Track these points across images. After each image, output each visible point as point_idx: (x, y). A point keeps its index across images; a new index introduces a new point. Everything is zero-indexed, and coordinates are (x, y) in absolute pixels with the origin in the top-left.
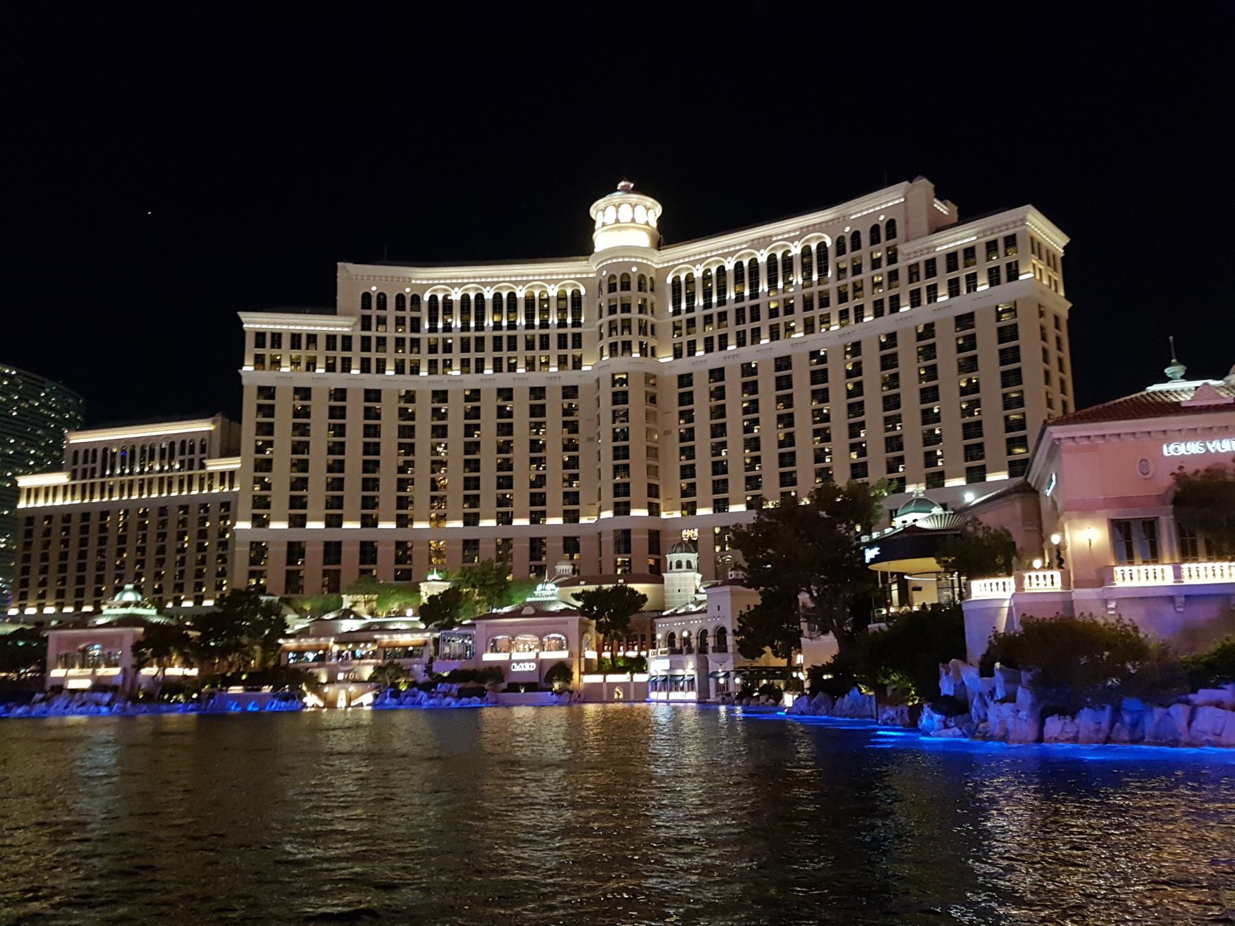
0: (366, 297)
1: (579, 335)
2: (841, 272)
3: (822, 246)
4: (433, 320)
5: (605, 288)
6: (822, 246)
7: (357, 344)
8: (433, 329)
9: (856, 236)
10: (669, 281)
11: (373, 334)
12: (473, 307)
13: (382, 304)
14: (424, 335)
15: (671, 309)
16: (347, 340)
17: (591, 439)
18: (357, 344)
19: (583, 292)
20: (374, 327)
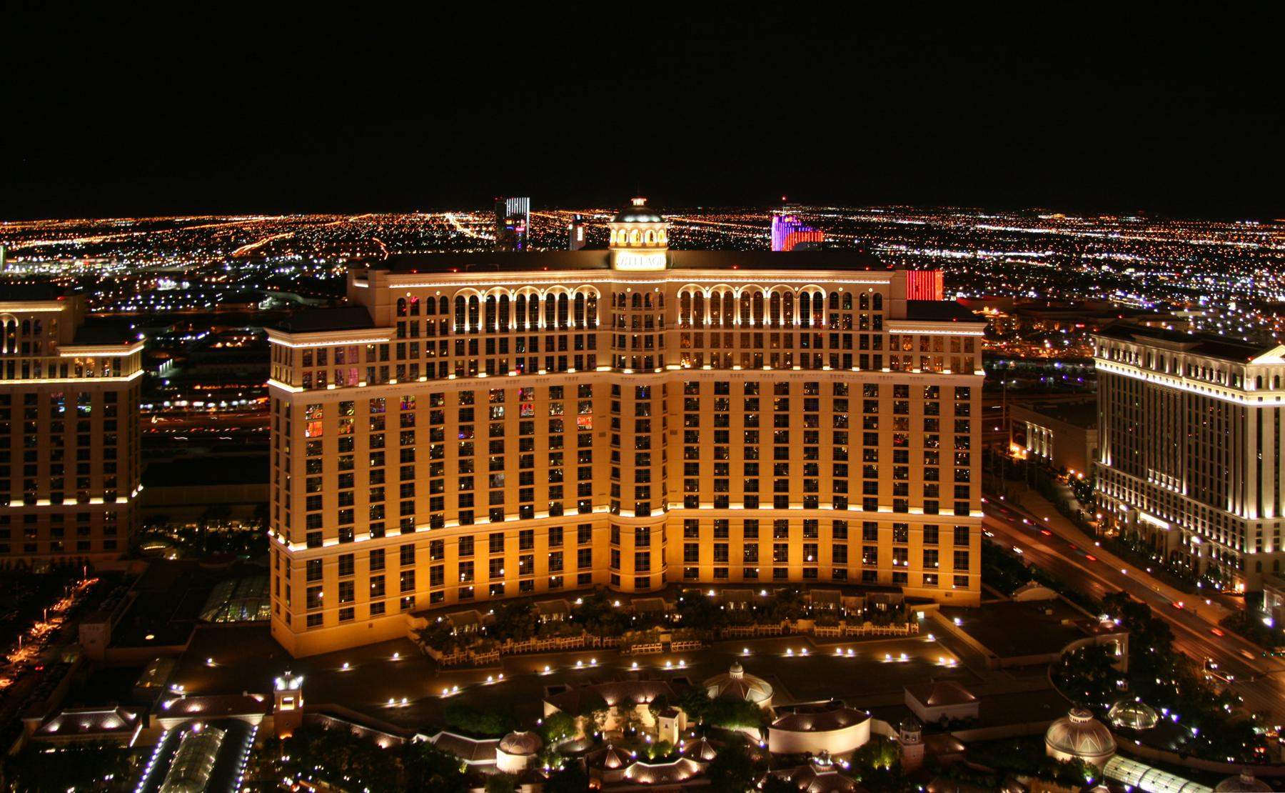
0: (401, 302)
1: (594, 336)
2: (833, 319)
3: (818, 295)
4: (461, 321)
5: (629, 302)
6: (818, 295)
7: (393, 353)
8: (461, 331)
9: (848, 298)
10: (679, 295)
11: (408, 341)
12: (499, 308)
13: (415, 310)
14: (452, 339)
15: (680, 322)
16: (384, 347)
17: (602, 435)
18: (393, 353)
19: (599, 296)
20: (408, 335)
